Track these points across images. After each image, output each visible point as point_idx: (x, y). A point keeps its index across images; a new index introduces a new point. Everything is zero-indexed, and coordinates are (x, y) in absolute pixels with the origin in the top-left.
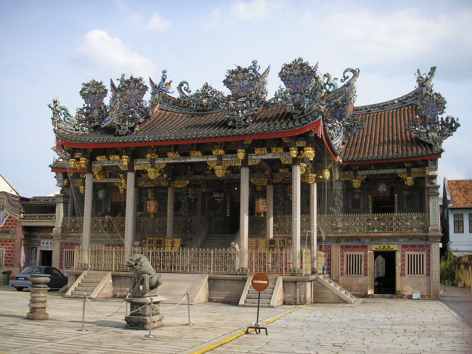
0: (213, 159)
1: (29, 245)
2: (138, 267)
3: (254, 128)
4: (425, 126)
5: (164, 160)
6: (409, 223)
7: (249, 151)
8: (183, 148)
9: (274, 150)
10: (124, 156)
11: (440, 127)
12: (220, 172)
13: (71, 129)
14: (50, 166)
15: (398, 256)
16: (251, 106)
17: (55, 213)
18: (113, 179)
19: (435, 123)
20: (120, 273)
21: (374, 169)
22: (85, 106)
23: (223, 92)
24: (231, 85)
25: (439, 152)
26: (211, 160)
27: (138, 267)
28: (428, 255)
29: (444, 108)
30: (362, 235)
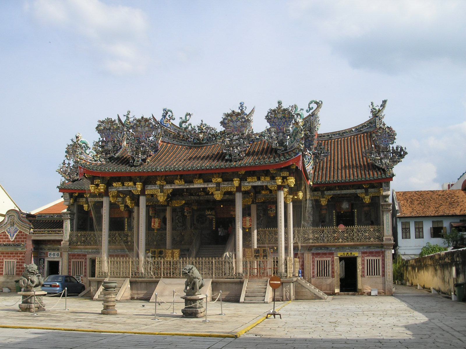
0: (213, 186)
1: (37, 257)
2: (190, 274)
3: (248, 161)
4: (379, 154)
6: (367, 234)
7: (243, 179)
8: (188, 177)
9: (263, 178)
10: (138, 183)
11: (391, 154)
13: (91, 160)
14: (58, 187)
15: (359, 261)
16: (244, 143)
17: (63, 228)
19: (387, 151)
20: (137, 279)
21: (338, 190)
22: (100, 140)
23: (216, 128)
24: (227, 125)
25: (391, 176)
26: (211, 186)
27: (190, 274)
28: (383, 259)
29: (395, 139)
30: (329, 244)
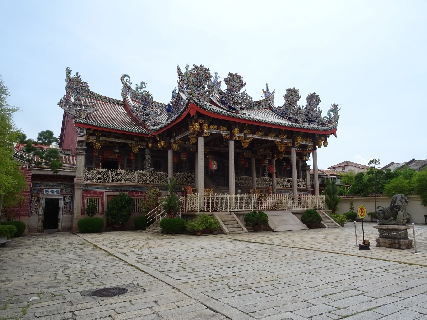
12: (282, 149)
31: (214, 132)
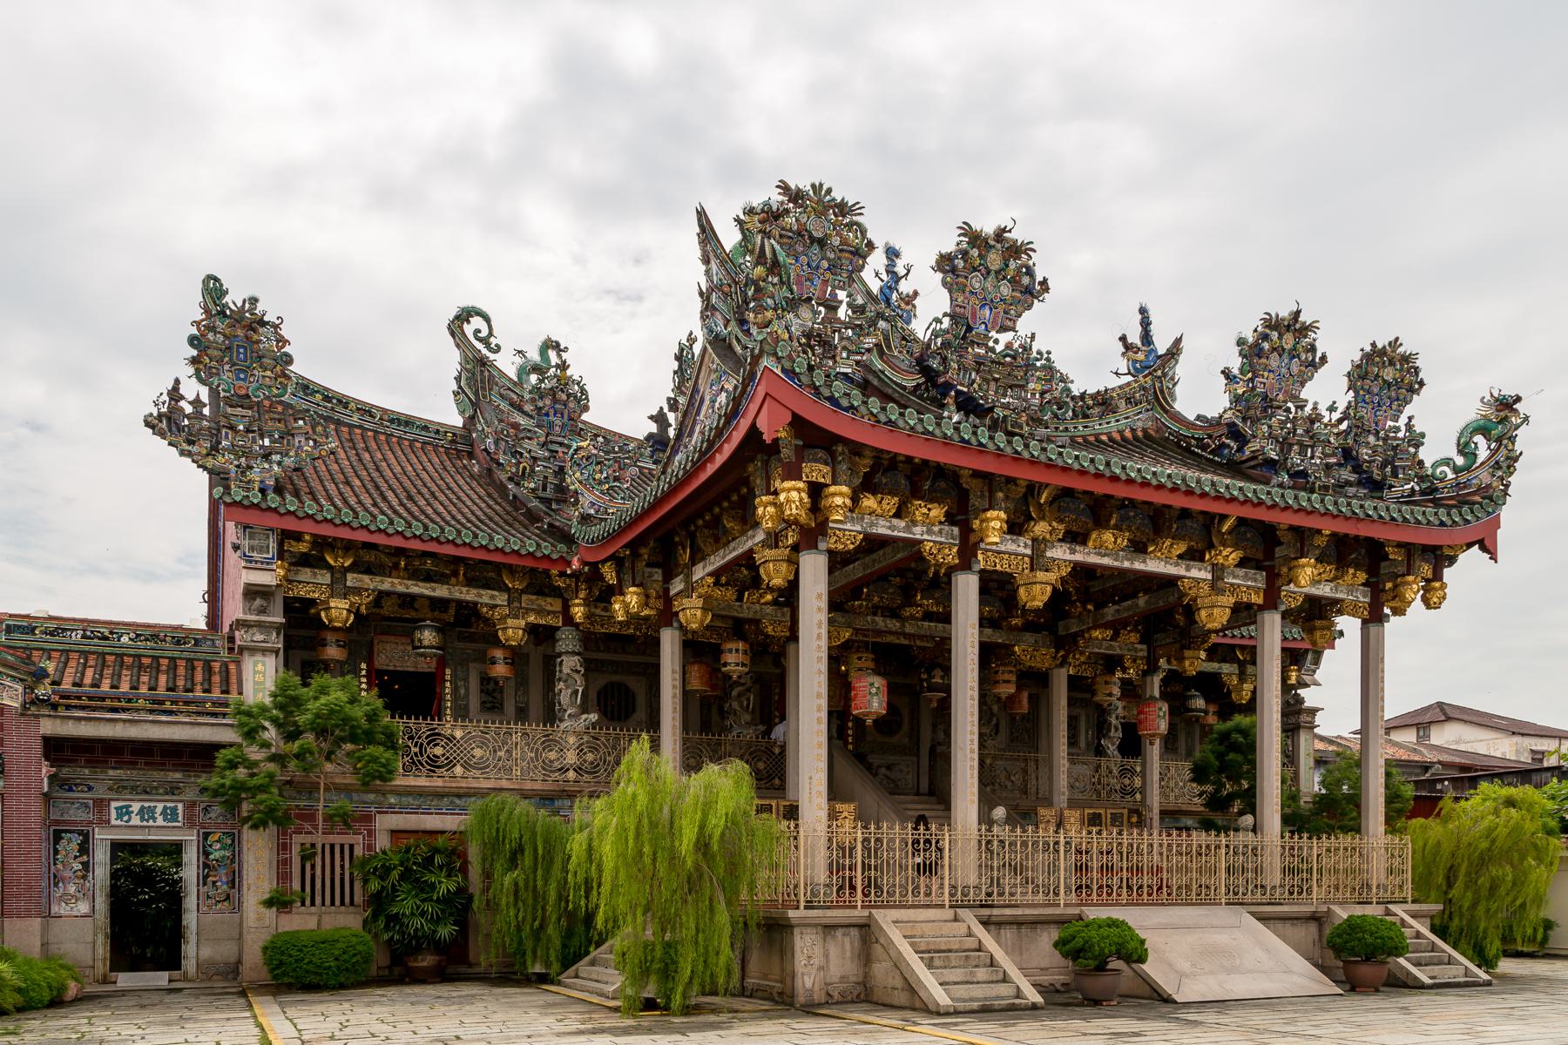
5: (1073, 552)
18: (474, 591)
31: (882, 531)
